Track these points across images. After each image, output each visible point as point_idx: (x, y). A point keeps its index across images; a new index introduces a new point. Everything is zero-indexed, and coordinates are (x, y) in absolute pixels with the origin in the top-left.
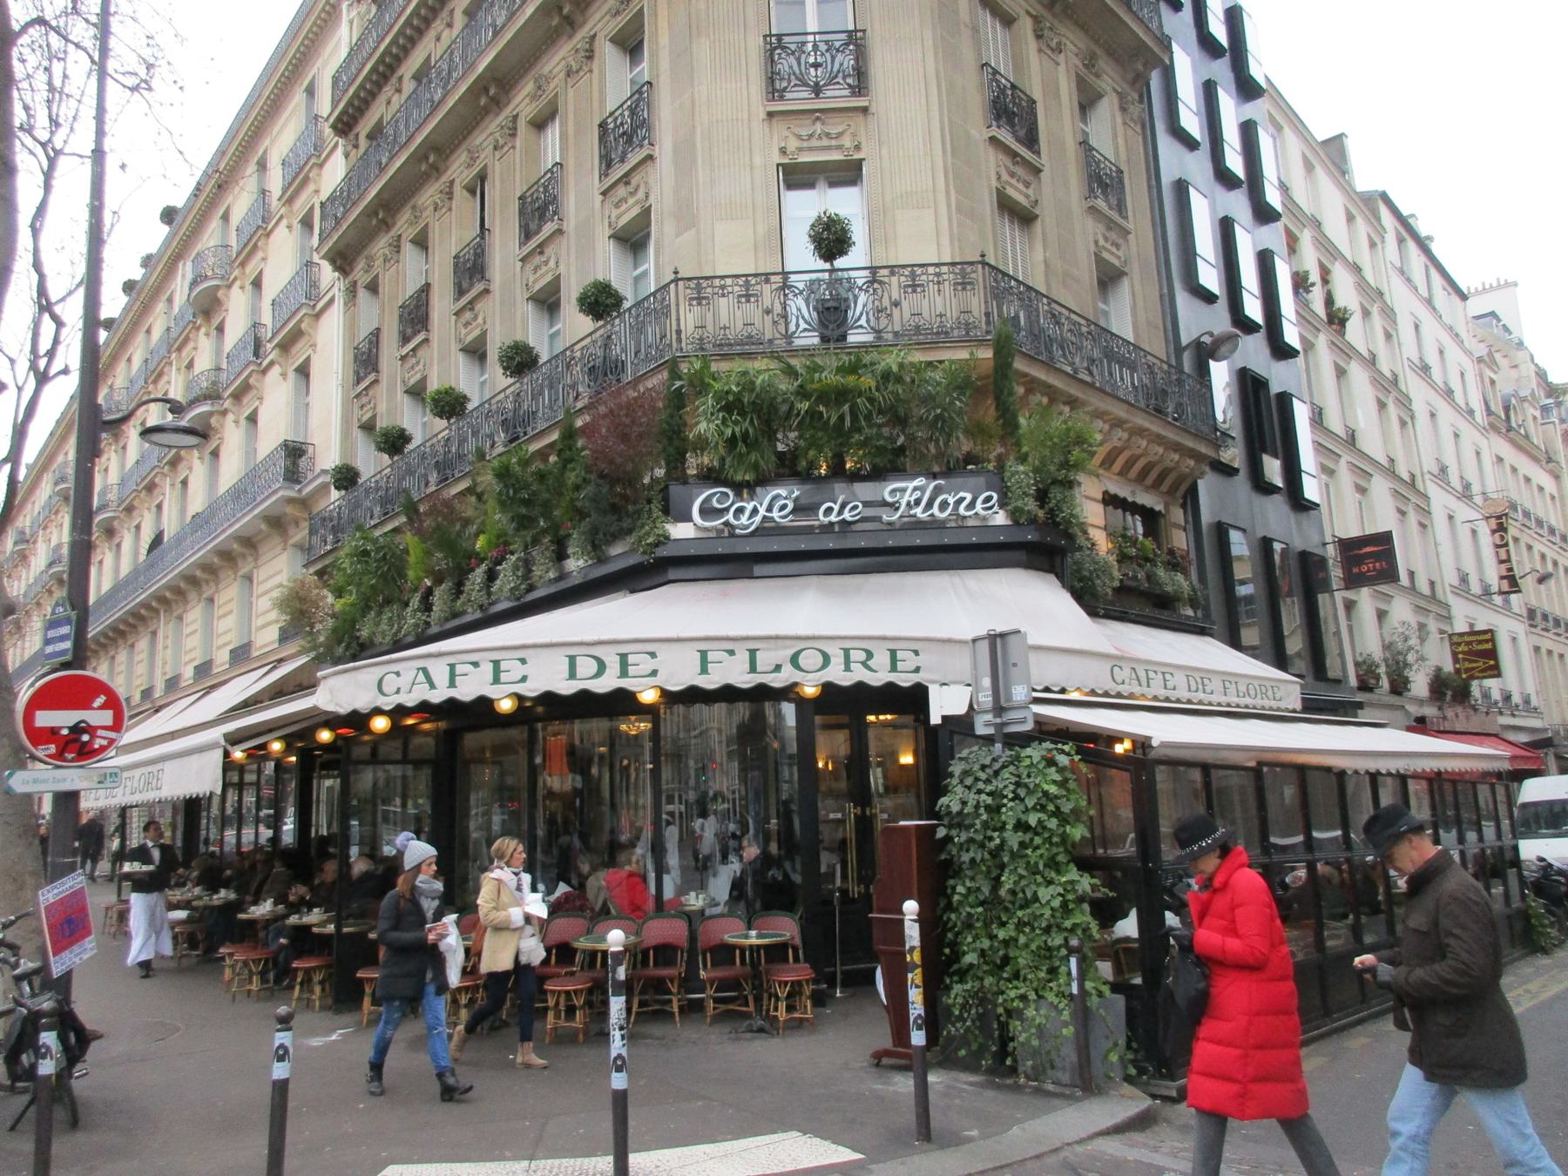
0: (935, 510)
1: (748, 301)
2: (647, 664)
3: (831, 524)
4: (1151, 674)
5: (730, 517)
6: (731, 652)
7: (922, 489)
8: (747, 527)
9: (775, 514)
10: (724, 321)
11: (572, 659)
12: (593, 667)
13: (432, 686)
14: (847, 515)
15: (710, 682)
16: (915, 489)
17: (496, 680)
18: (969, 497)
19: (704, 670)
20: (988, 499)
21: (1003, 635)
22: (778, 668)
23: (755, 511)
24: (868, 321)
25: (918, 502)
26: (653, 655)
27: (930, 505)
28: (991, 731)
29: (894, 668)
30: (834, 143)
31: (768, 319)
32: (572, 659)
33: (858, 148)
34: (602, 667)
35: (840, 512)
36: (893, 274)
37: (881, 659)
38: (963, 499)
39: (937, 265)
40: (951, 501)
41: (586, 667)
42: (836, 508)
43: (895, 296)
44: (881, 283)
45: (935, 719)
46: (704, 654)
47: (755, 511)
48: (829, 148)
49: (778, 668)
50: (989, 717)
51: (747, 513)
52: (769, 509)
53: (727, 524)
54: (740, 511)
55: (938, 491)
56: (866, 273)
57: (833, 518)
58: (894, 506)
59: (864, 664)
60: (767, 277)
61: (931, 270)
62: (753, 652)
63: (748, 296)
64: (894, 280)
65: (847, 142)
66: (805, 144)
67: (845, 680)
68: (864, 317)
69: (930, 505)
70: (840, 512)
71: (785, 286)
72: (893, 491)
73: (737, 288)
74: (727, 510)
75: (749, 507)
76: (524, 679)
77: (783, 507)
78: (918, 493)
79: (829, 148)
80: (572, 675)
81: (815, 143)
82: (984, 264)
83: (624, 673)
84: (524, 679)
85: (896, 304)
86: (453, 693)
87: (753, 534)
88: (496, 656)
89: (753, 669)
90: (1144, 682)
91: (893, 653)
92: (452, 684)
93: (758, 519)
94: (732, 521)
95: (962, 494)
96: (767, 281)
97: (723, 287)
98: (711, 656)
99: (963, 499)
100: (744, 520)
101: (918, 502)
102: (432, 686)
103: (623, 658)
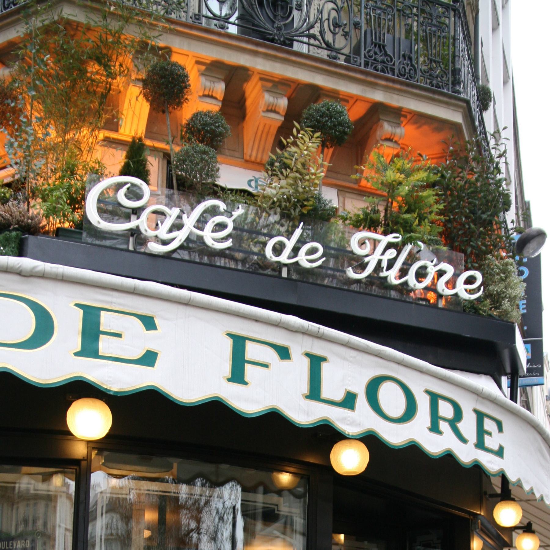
0: (411, 278)
2: (137, 341)
3: (280, 265)
6: (284, 353)
8: (165, 243)
14: (303, 259)
15: (248, 401)
16: (389, 246)
19: (237, 376)
22: (349, 401)
23: (177, 226)
25: (391, 264)
26: (149, 323)
35: (296, 251)
37: (468, 426)
42: (290, 244)
46: (239, 343)
51: (168, 222)
53: (135, 232)
57: (284, 258)
67: (434, 445)
70: (296, 251)
72: (362, 243)
74: (137, 212)
77: (221, 226)
78: (392, 253)
83: (89, 347)
87: (167, 256)
89: (314, 393)
91: (480, 416)
93: (181, 236)
94: (147, 231)
98: (252, 351)
101: (391, 264)
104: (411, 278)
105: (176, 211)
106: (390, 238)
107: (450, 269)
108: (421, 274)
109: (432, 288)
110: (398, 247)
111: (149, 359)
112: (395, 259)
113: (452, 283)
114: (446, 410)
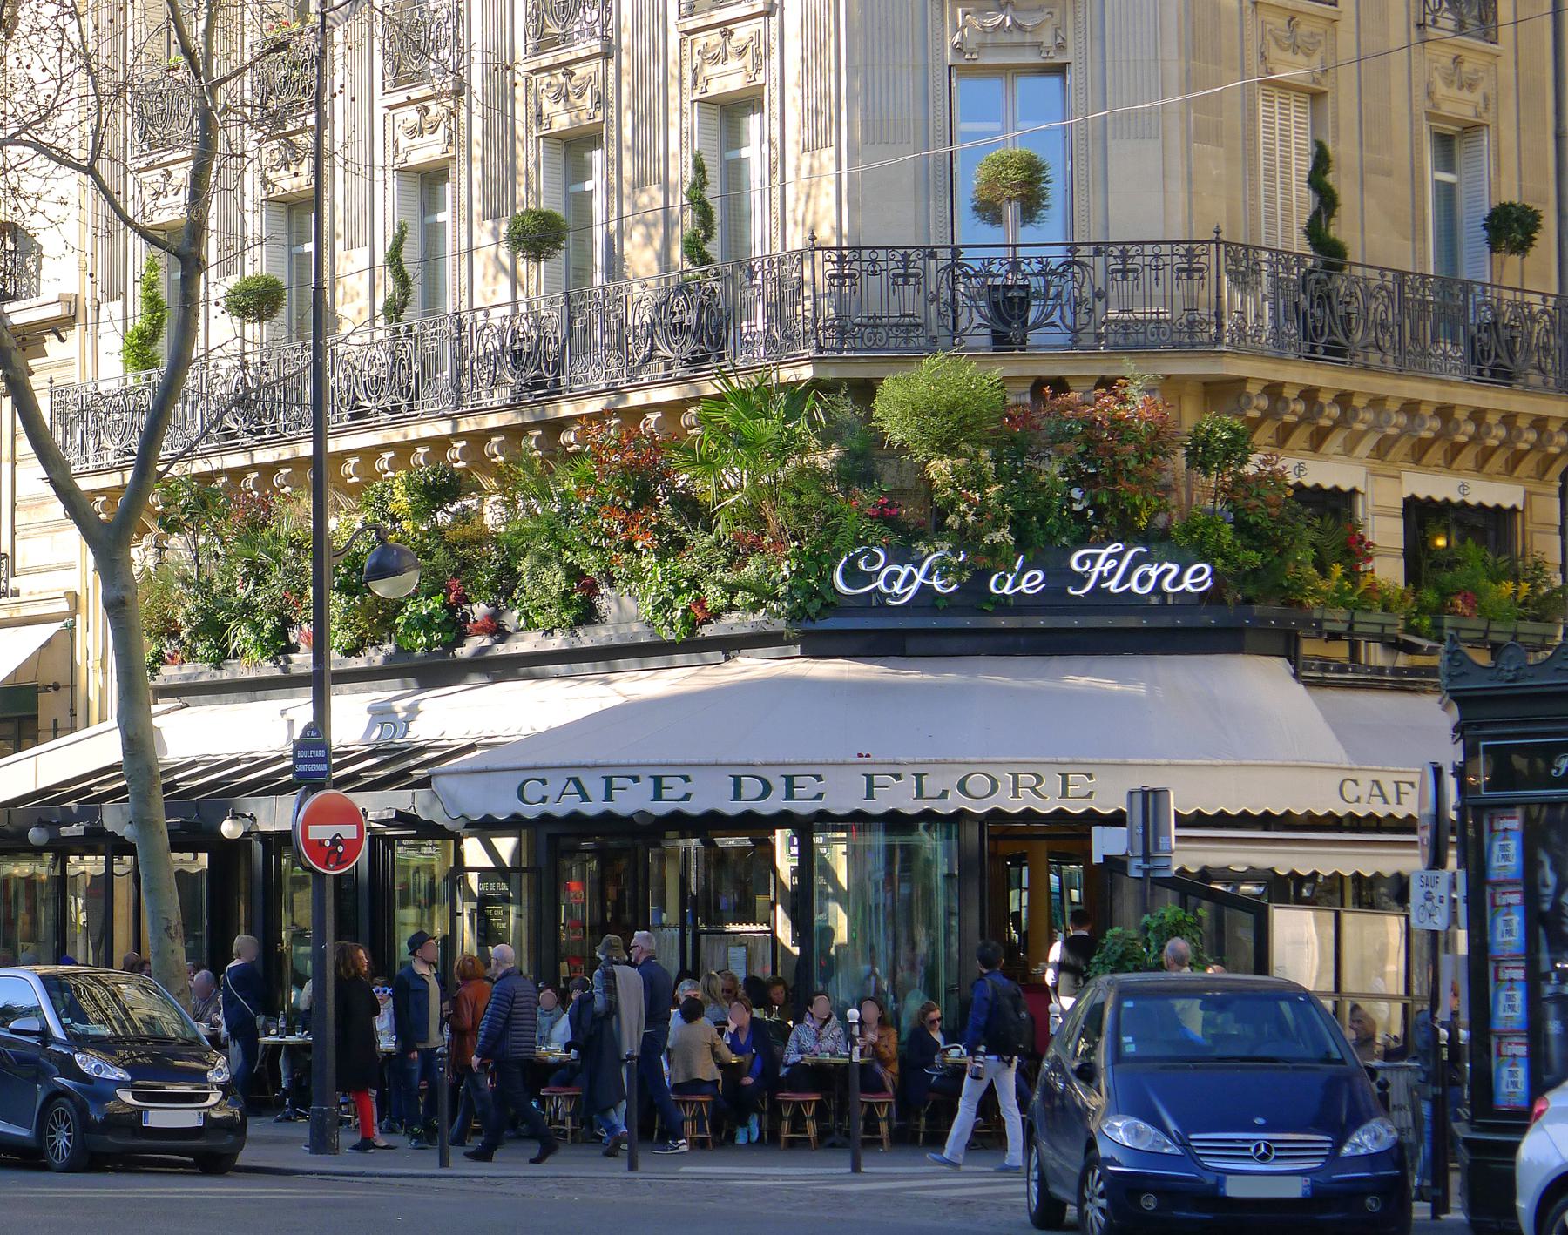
0: (1133, 584)
1: (906, 283)
4: (1404, 788)
5: (880, 583)
7: (1118, 557)
9: (936, 583)
10: (875, 309)
11: (737, 781)
12: (759, 787)
13: (585, 798)
14: (1023, 586)
16: (1110, 556)
17: (658, 796)
18: (1175, 568)
19: (870, 796)
20: (1200, 572)
21: (1155, 791)
22: (944, 794)
23: (910, 578)
24: (1062, 318)
25: (1112, 573)
27: (1126, 578)
28: (1140, 875)
29: (1064, 795)
30: (1028, 38)
31: (933, 308)
32: (737, 781)
33: (1061, 47)
34: (767, 789)
36: (1097, 253)
37: (1052, 783)
38: (1167, 571)
39: (1156, 243)
40: (1154, 572)
41: (752, 787)
43: (1099, 284)
44: (1080, 264)
45: (1097, 859)
46: (870, 778)
47: (910, 578)
48: (1022, 45)
49: (944, 794)
50: (1140, 862)
51: (901, 580)
52: (928, 575)
54: (894, 576)
55: (1137, 561)
56: (1060, 251)
57: (1005, 590)
58: (1081, 580)
59: (1033, 789)
60: (931, 253)
61: (1148, 249)
62: (919, 777)
63: (906, 276)
64: (1099, 260)
65: (1047, 39)
66: (989, 39)
67: (1015, 807)
68: (1057, 313)
69: (1126, 578)
71: (955, 263)
72: (1081, 562)
73: (892, 265)
74: (878, 573)
75: (904, 571)
76: (687, 797)
79: (1022, 45)
80: (737, 796)
81: (1004, 38)
82: (1217, 242)
83: (789, 796)
84: (687, 797)
85: (1099, 295)
86: (608, 806)
88: (657, 772)
89: (920, 795)
90: (1392, 798)
92: (608, 798)
93: (914, 587)
95: (1167, 565)
96: (933, 256)
97: (874, 262)
99: (1167, 571)
100: (897, 588)
101: (1112, 573)
102: (585, 798)
103: (789, 780)
104: (1133, 584)
105: (908, 568)
106: (1110, 549)
107: (1175, 568)
108: (1144, 580)
109: (1158, 589)
110: (1118, 557)
111: (819, 796)
112: (1117, 568)
113: (1177, 581)
114: (1027, 780)
